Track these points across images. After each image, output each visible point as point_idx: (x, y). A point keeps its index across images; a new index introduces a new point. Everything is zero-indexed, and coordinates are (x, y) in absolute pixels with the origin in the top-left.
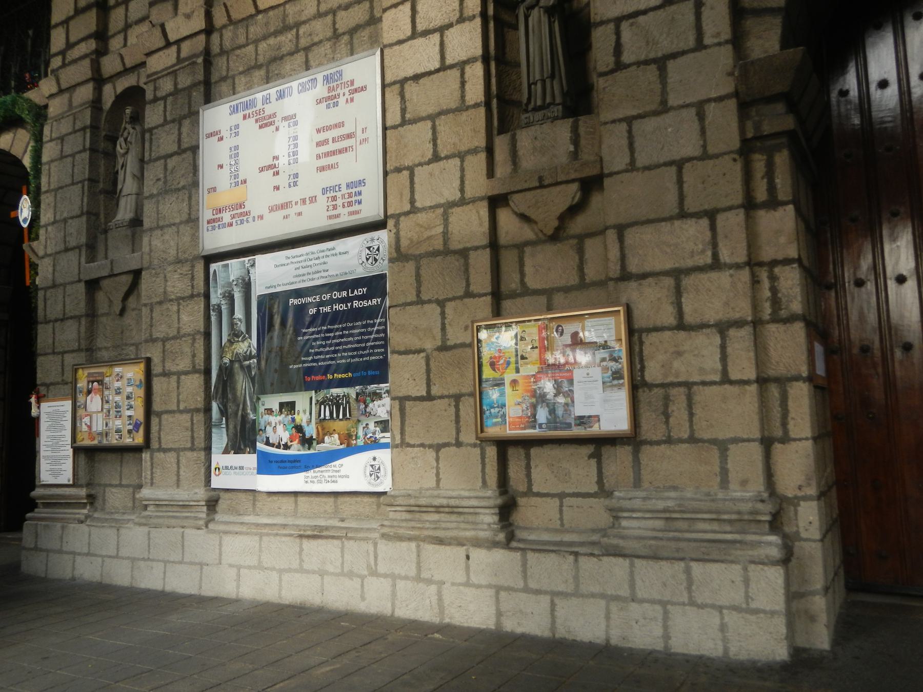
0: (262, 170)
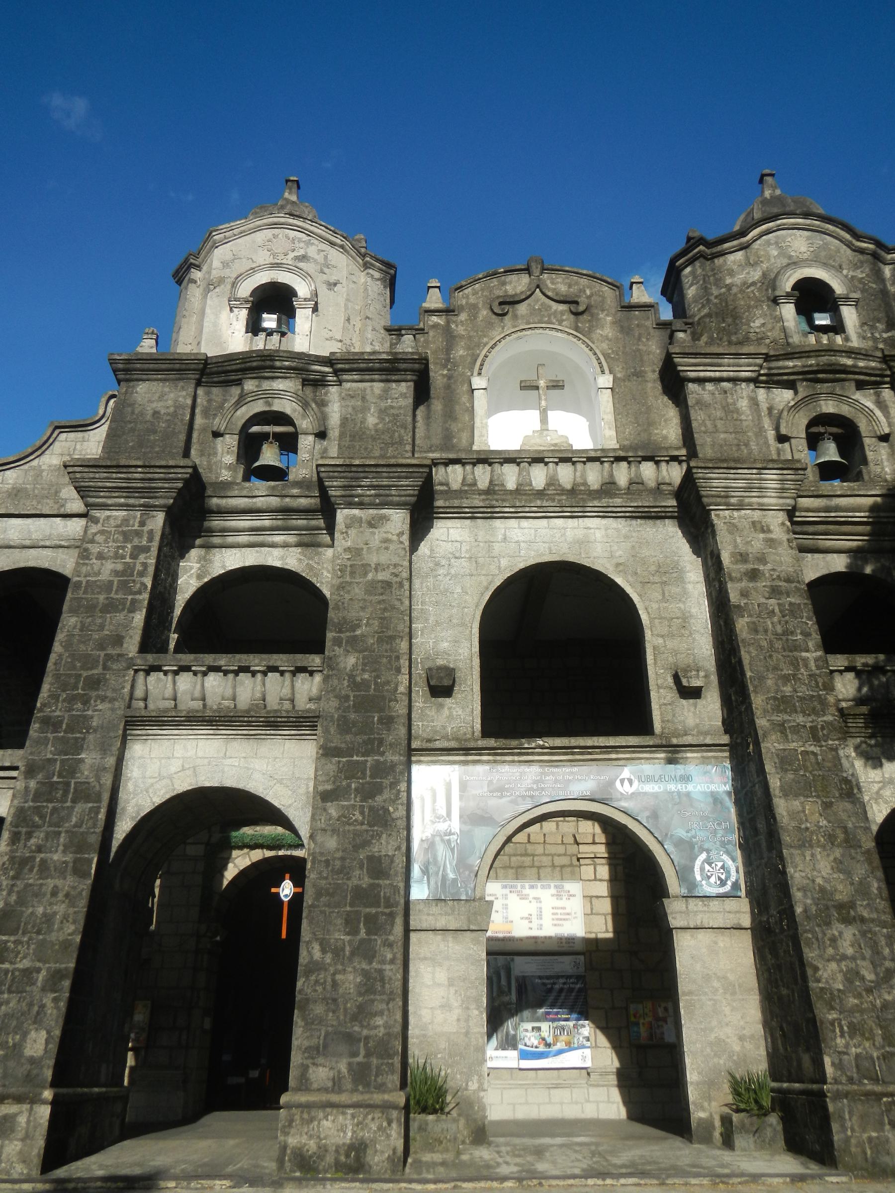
0: (522, 918)
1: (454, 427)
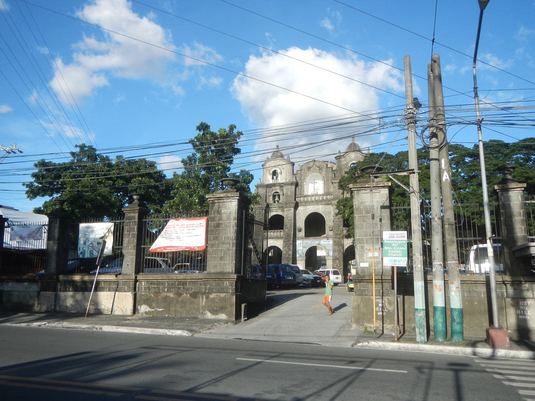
1: (302, 191)
